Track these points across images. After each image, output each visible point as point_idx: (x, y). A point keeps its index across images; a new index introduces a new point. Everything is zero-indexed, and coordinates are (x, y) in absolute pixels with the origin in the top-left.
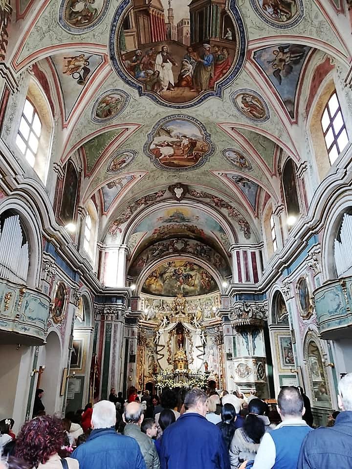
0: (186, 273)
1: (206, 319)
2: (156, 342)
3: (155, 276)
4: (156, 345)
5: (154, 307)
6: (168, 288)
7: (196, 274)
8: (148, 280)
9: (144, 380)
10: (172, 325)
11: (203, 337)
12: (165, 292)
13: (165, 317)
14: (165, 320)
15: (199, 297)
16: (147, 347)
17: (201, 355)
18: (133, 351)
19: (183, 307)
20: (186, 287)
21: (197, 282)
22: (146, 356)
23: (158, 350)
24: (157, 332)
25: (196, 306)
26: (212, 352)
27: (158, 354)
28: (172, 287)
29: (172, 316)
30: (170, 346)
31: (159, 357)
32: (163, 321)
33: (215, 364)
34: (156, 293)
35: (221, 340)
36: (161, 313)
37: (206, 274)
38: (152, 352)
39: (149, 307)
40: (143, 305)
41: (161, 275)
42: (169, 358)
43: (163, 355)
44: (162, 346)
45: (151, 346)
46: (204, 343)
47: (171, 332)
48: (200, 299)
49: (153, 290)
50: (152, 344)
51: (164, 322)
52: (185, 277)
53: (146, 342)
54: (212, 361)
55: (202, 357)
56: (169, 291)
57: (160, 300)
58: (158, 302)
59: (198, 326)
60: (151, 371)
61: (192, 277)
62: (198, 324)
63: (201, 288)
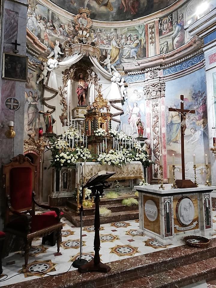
4: (43, 86)
5: (38, 18)
10: (71, 60)
13: (58, 43)
14: (57, 49)
20: (94, 4)
23: (45, 97)
25: (109, 40)
27: (46, 105)
35: (160, 91)
38: (34, 98)
42: (63, 115)
43: (54, 109)
44: (52, 90)
45: (32, 87)
47: (66, 72)
48: (116, 29)
57: (49, 10)
62: (113, 67)
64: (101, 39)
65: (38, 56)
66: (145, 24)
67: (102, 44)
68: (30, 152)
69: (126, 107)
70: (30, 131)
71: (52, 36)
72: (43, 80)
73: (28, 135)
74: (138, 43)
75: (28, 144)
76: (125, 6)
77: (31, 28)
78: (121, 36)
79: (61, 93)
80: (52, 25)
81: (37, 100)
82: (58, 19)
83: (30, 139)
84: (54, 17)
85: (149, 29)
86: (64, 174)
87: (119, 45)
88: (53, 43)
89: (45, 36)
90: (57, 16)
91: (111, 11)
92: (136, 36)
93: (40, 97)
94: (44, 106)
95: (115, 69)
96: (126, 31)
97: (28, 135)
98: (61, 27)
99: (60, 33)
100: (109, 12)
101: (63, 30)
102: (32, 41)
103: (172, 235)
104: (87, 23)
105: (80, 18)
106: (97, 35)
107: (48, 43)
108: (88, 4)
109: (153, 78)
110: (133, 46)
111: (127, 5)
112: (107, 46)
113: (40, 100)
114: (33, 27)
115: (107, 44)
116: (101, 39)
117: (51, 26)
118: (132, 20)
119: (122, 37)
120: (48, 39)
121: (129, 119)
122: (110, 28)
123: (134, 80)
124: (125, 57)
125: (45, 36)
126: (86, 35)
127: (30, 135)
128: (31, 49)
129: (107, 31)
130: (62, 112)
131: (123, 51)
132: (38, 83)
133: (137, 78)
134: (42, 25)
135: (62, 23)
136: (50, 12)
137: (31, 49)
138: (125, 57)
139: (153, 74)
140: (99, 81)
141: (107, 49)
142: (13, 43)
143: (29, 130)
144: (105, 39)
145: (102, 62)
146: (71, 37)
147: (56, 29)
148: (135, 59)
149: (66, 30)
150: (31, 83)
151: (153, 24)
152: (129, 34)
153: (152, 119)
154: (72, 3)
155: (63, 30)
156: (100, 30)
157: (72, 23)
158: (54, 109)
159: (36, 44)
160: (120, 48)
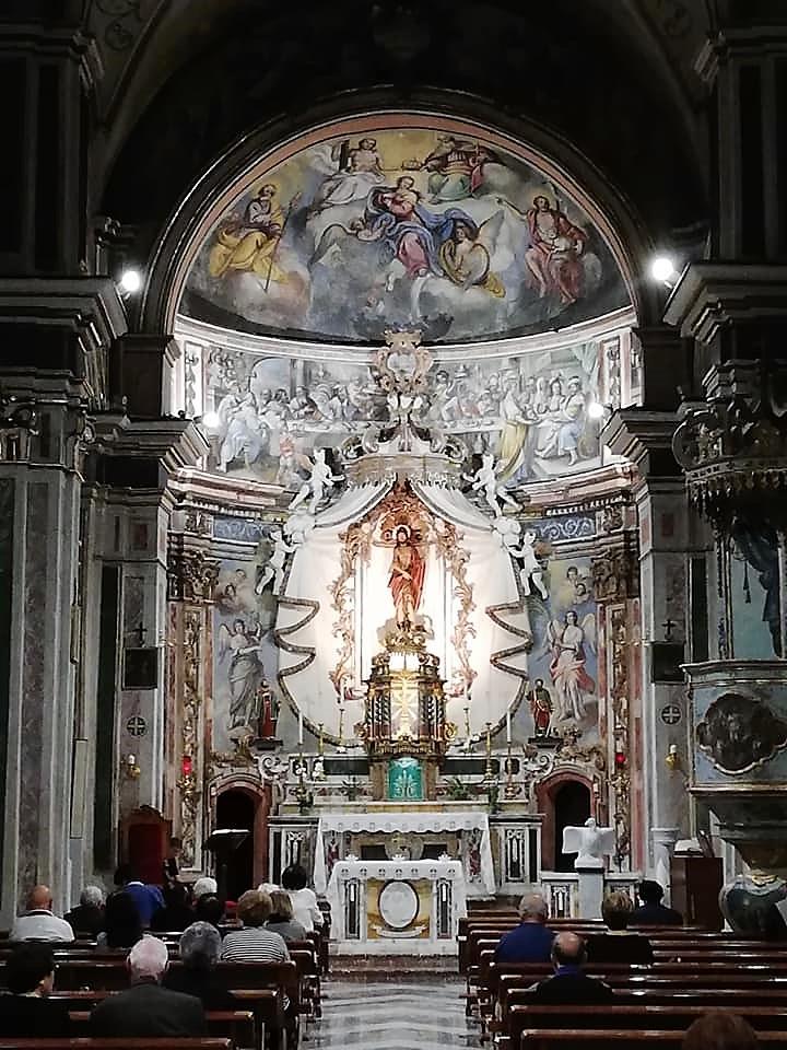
0: (439, 210)
1: (547, 468)
2: (270, 586)
3: (262, 228)
4: (274, 601)
6: (339, 295)
7: (502, 212)
8: (220, 249)
9: (206, 778)
11: (531, 563)
13: (320, 456)
14: (321, 471)
15: (514, 347)
16: (225, 610)
17: (517, 651)
18: (141, 630)
19: (419, 402)
20: (442, 288)
21: (501, 261)
22: (216, 660)
23: (278, 626)
24: (277, 535)
26: (572, 636)
28: (357, 288)
29: (360, 452)
30: (347, 606)
31: (287, 660)
33: (588, 698)
34: (268, 322)
37: (557, 214)
39: (230, 398)
40: (197, 387)
41: (299, 220)
42: (340, 665)
44: (301, 603)
45: (242, 606)
46: (535, 591)
49: (252, 306)
50: (248, 595)
52: (437, 231)
53: (213, 583)
54: (572, 685)
55: (520, 662)
56: (344, 310)
57: (293, 361)
58: (277, 374)
59: (501, 501)
60: (245, 734)
61: (473, 233)
63: (528, 295)
64: (468, 401)
65: (259, 515)
66: (598, 340)
67: (471, 417)
68: (236, 784)
69: (546, 626)
70: (237, 728)
72: (273, 579)
73: (232, 740)
74: (581, 405)
75: (232, 765)
76: (541, 278)
77: (240, 441)
78: (532, 381)
79: (334, 602)
80: (305, 401)
81: (259, 639)
83: (235, 751)
84: (310, 373)
85: (606, 359)
86: (292, 842)
87: (524, 415)
89: (282, 446)
90: (321, 367)
91: (501, 299)
92: (575, 380)
93: (266, 628)
94: (278, 656)
95: (507, 498)
96: (546, 363)
97: (232, 740)
98: (335, 395)
99: (330, 417)
100: (493, 303)
101: (342, 402)
102: (233, 495)
103: (359, 938)
104: (418, 362)
105: (391, 356)
106: (456, 387)
107: (294, 461)
108: (425, 293)
109: (610, 535)
110: (567, 414)
111: (547, 276)
112: (487, 420)
113: (266, 636)
115: (487, 414)
116: (470, 398)
118: (556, 330)
119: (534, 385)
121: (553, 667)
122: (498, 361)
123: (568, 535)
124: (542, 454)
125: (282, 446)
126: (412, 403)
127: (236, 741)
129: (488, 367)
130: (338, 659)
131: (537, 431)
132: (260, 592)
133: (577, 526)
135: (338, 383)
136: (299, 364)
138: (542, 454)
139: (610, 518)
140: (460, 544)
141: (487, 432)
142: (136, 630)
143: (234, 727)
144: (481, 400)
145: (471, 479)
146: (368, 414)
147: (320, 408)
148: (573, 460)
149: (352, 399)
150: (240, 599)
151: (616, 342)
152: (554, 374)
153: (610, 668)
154: (369, 305)
155: (342, 402)
156: (466, 370)
157: (373, 368)
158: (313, 655)
160: (529, 422)
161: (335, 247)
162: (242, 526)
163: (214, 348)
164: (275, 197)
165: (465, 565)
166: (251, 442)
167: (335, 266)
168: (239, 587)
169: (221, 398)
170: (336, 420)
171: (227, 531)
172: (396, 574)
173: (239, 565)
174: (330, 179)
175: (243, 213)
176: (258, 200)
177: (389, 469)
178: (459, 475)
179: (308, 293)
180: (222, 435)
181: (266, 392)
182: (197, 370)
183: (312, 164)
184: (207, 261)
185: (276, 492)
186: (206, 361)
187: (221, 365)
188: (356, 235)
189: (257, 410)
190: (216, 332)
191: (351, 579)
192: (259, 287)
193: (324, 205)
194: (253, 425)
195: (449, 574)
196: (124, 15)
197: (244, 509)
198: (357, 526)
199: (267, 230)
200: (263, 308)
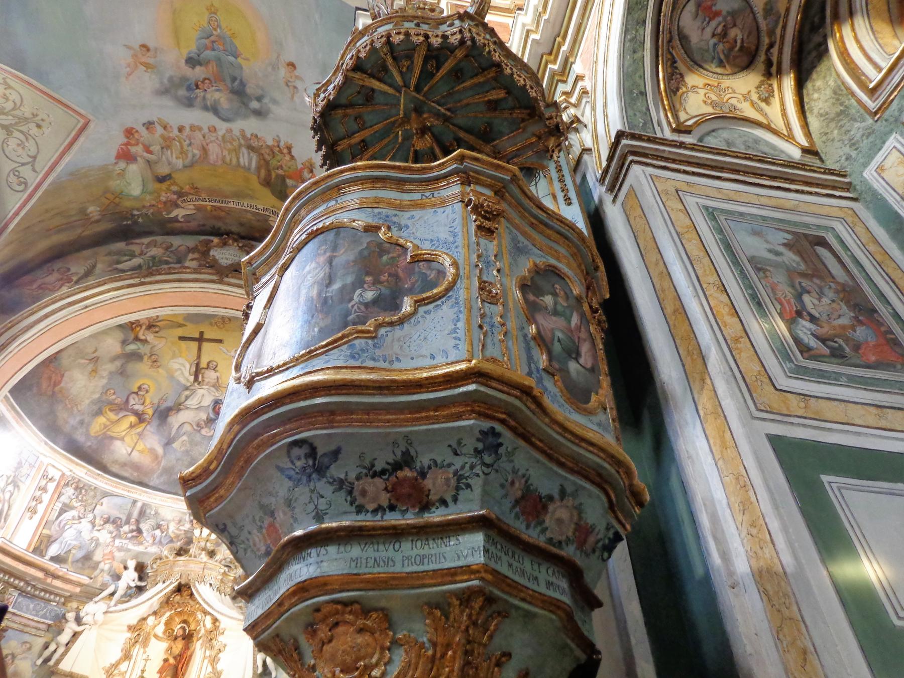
2: (48, 659)
8: (102, 420)
12: (164, 478)
13: (132, 564)
14: (130, 577)
24: (71, 616)
32: (118, 577)
36: (120, 549)
40: (46, 498)
41: (163, 414)
49: (115, 462)
51: (122, 585)
65: (63, 600)
71: (128, 550)
72: (55, 651)
82: (156, 513)
88: (122, 566)
99: (151, 542)
101: (163, 533)
102: (40, 575)
107: (112, 567)
114: (74, 543)
117: (132, 531)
120: (113, 558)
128: (42, 590)
134: (104, 536)
137: (42, 590)
147: (145, 534)
149: (170, 531)
155: (163, 533)
159: (55, 577)
161: (185, 438)
162: (45, 607)
163: (74, 478)
164: (150, 394)
165: (220, 655)
166: (80, 547)
167: (183, 448)
168: (19, 657)
169: (66, 511)
170: (153, 544)
171: (28, 609)
172: (166, 660)
173: (27, 638)
174: (187, 388)
175: (124, 400)
176: (136, 393)
177: (177, 569)
178: (230, 584)
179: (159, 463)
180: (55, 536)
181: (106, 516)
182: (51, 487)
183: (177, 374)
184: (89, 425)
185: (83, 582)
186: (63, 483)
187: (76, 489)
188: (199, 431)
189: (94, 526)
190: (77, 464)
191: (126, 663)
192: (125, 452)
193: (181, 407)
194: (86, 536)
195: (206, 661)
196: (23, 164)
197: (51, 593)
198: (144, 619)
199: (140, 417)
200: (124, 465)
